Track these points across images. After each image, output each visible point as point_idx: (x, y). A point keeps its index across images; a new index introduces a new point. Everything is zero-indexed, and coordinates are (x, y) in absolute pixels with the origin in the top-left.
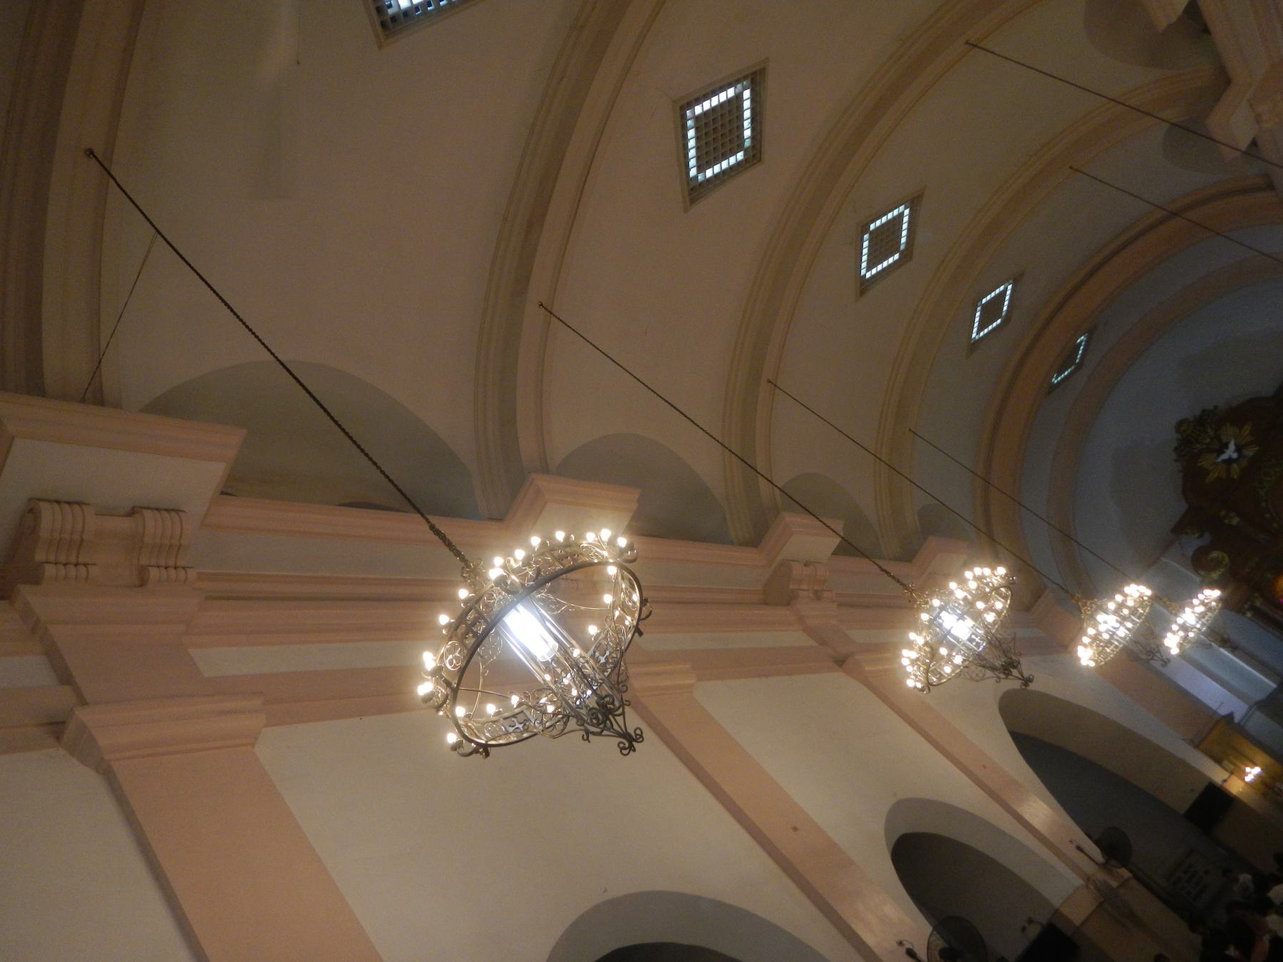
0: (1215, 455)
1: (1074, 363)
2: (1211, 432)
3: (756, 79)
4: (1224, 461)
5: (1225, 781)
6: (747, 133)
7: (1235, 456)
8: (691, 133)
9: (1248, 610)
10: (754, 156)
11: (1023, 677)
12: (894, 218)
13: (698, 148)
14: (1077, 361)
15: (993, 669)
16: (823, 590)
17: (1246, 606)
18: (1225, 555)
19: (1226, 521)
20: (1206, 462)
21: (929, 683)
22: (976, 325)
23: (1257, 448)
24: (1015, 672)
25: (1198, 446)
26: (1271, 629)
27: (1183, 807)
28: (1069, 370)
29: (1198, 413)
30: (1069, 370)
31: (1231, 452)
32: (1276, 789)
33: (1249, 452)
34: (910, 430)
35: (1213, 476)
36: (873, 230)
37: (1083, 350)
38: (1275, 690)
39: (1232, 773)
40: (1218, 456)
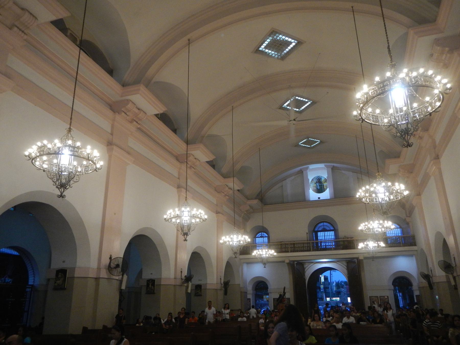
3: (299, 43)
11: (186, 238)
12: (305, 101)
16: (193, 168)
21: (168, 220)
22: (302, 142)
24: (185, 236)
34: (259, 148)
36: (297, 99)
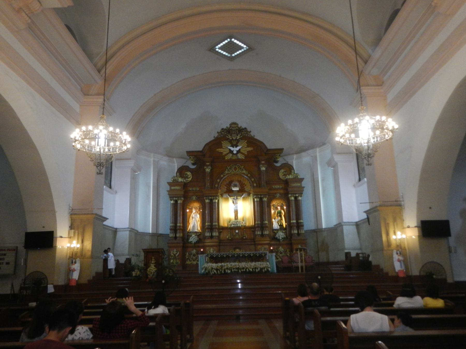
1: (231, 54)
2: (238, 137)
4: (230, 150)
5: (61, 237)
7: (235, 152)
9: (174, 200)
14: (233, 55)
17: (175, 199)
18: (192, 177)
19: (205, 167)
23: (244, 158)
25: (230, 136)
27: (29, 231)
28: (227, 54)
29: (243, 127)
30: (227, 54)
31: (235, 150)
32: (74, 261)
33: (240, 156)
35: (220, 150)
37: (240, 53)
38: (150, 233)
39: (70, 238)
40: (231, 146)
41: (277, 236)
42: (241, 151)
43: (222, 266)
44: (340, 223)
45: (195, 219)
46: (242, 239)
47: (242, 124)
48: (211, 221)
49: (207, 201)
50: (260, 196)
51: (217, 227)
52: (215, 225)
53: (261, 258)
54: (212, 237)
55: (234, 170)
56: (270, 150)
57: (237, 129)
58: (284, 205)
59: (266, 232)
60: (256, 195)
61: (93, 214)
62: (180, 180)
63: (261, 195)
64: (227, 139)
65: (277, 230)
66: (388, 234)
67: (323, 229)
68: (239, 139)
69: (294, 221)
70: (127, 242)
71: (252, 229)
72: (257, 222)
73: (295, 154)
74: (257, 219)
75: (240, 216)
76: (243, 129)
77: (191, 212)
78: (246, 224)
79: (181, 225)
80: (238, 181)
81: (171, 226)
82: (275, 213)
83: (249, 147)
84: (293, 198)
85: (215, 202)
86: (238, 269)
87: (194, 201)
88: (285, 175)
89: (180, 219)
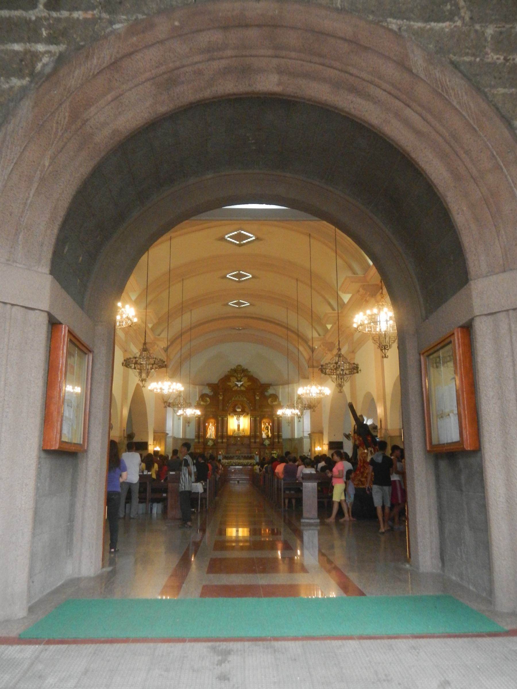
0: (235, 380)
3: (257, 239)
4: (236, 384)
5: (150, 445)
6: (244, 242)
7: (239, 385)
8: (236, 233)
10: (240, 245)
13: (233, 235)
15: (163, 400)
20: (233, 379)
25: (236, 374)
26: (196, 426)
31: (239, 384)
33: (242, 388)
35: (229, 384)
38: (181, 438)
41: (265, 443)
42: (244, 385)
43: (230, 462)
44: (302, 437)
45: (211, 430)
46: (242, 444)
47: (245, 365)
48: (222, 432)
49: (220, 419)
50: (254, 417)
51: (226, 436)
52: (225, 435)
53: (251, 458)
54: (222, 442)
55: (238, 398)
56: (263, 384)
57: (241, 370)
58: (270, 422)
59: (258, 440)
60: (252, 416)
61: (164, 433)
62: (202, 403)
63: (255, 416)
64: (235, 376)
65: (265, 439)
66: (315, 448)
67: (294, 439)
68: (243, 376)
69: (276, 434)
70: (171, 445)
71: (249, 437)
72: (252, 434)
73: (282, 385)
74: (252, 431)
75: (241, 428)
76: (245, 370)
77: (209, 425)
78: (245, 434)
79: (203, 434)
80: (240, 404)
81: (195, 435)
82: (264, 427)
83: (249, 382)
84: (276, 418)
85: (225, 420)
86: (239, 463)
87: (211, 418)
88: (272, 402)
89: (202, 430)
